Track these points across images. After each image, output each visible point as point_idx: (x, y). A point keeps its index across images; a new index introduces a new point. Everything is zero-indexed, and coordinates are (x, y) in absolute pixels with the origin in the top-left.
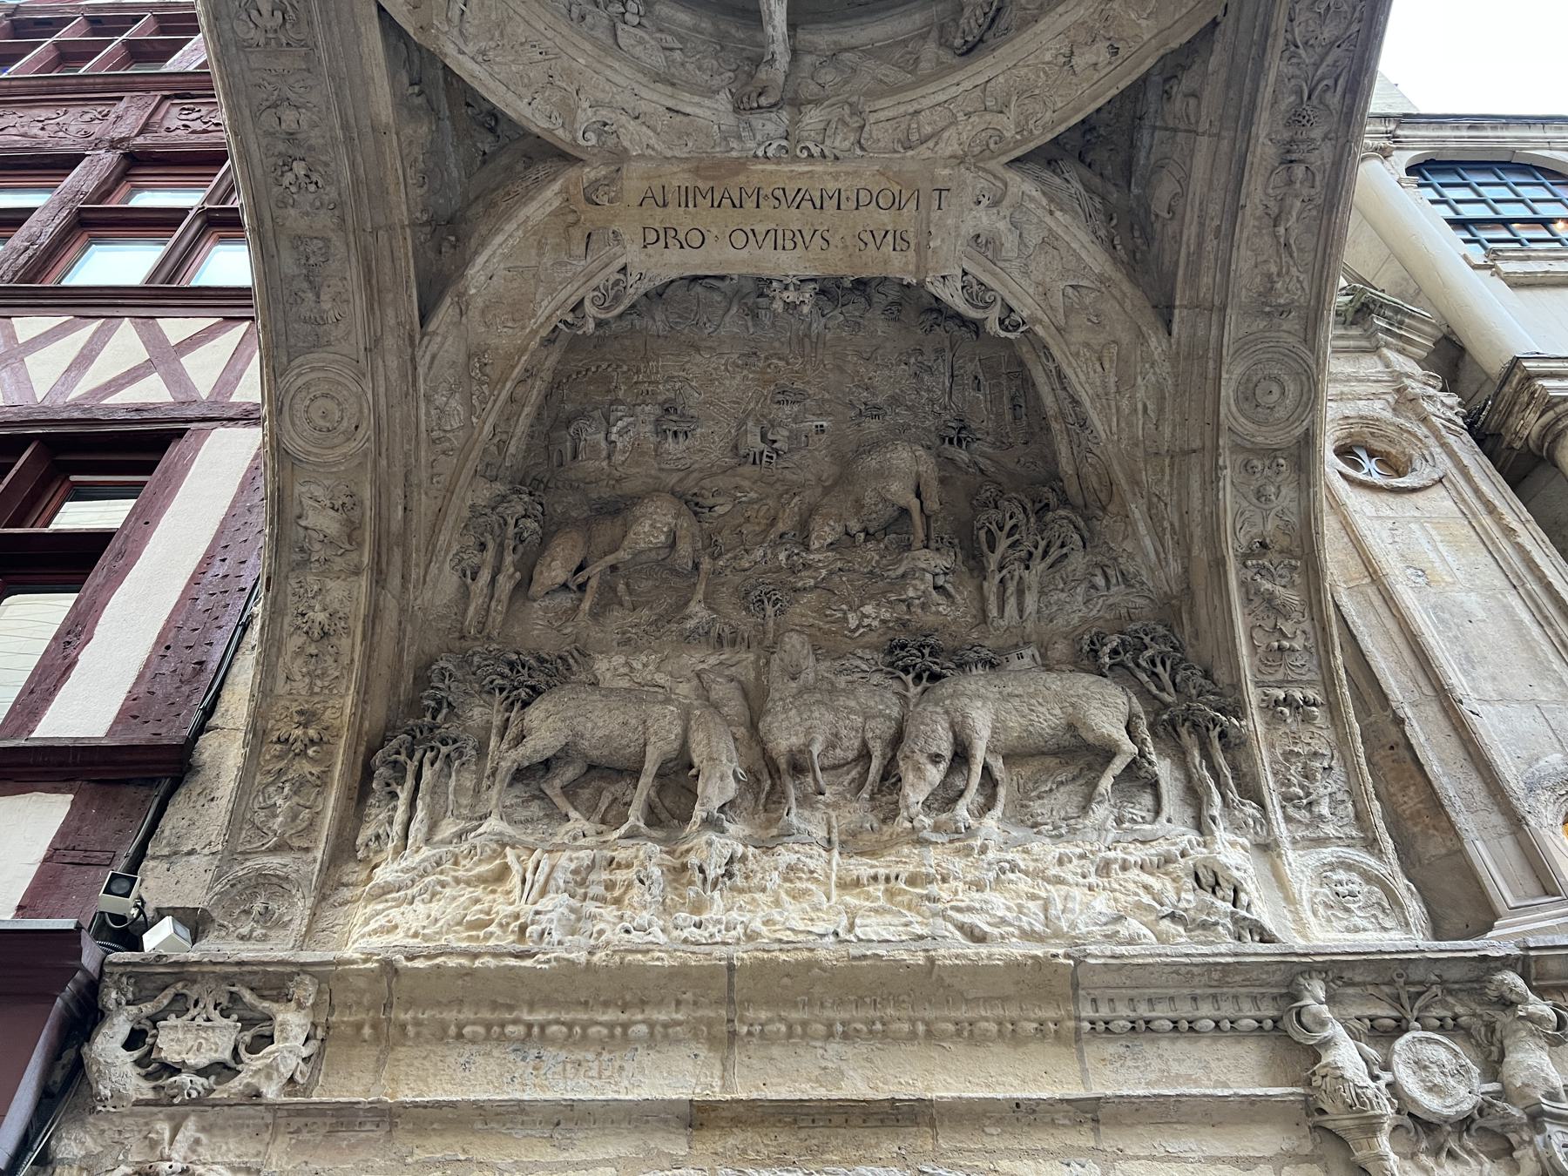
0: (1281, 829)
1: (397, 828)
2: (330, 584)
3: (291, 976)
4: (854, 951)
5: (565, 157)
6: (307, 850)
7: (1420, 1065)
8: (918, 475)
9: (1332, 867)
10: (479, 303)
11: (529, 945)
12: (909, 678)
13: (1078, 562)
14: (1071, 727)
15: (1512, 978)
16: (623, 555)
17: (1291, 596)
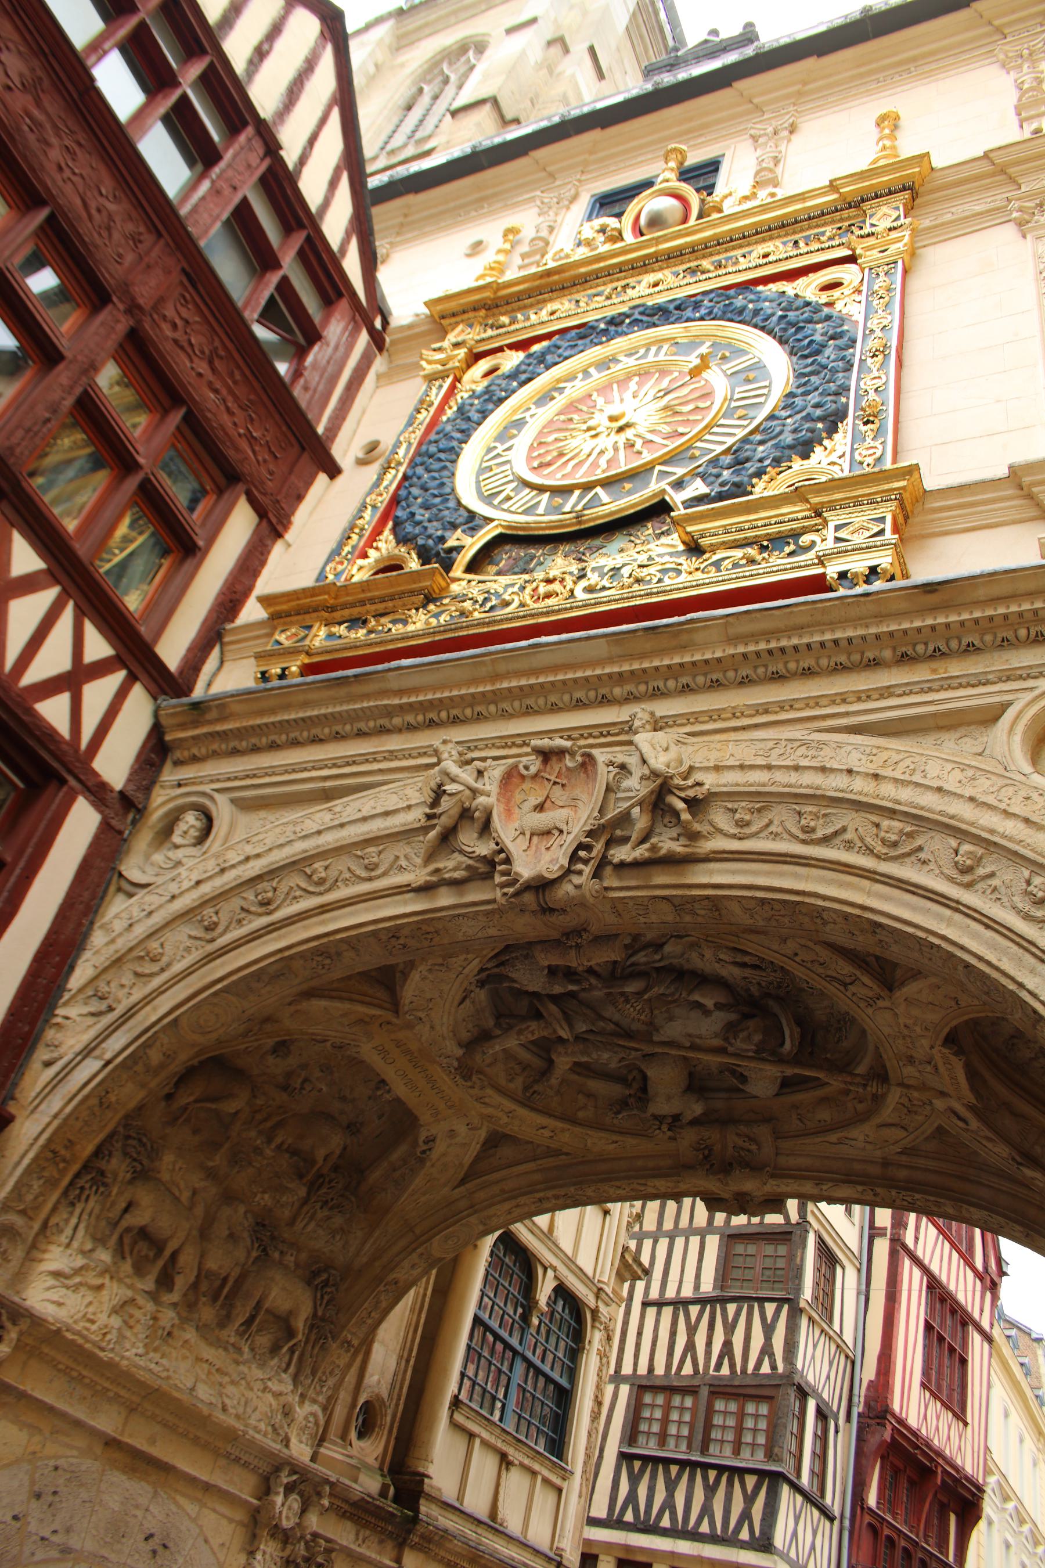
0: (311, 1393)
1: (68, 1231)
2: (130, 1085)
3: (23, 1316)
4: (194, 1402)
5: (395, 1007)
6: (31, 1219)
7: (290, 1508)
8: (332, 1153)
9: (311, 1414)
10: (299, 1007)
11: (104, 1344)
12: (256, 1245)
13: (338, 1220)
14: (290, 1312)
15: (327, 1488)
16: (214, 1106)
17: (384, 1305)
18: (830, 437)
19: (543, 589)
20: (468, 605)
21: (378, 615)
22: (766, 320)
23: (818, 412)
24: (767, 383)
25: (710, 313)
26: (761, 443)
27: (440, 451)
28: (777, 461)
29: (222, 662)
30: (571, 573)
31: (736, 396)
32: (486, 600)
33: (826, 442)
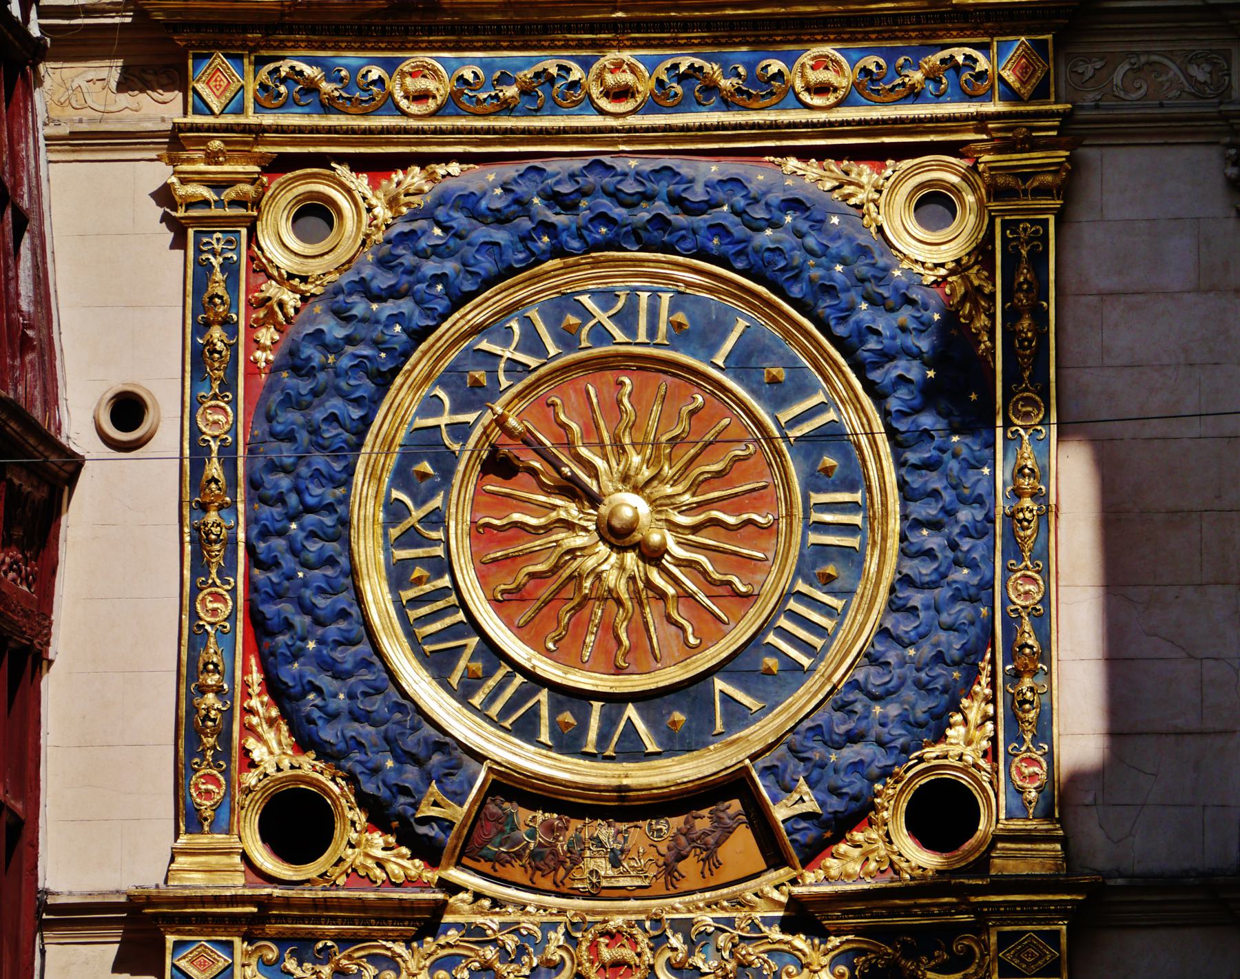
18: (970, 695)
19: (606, 954)
20: (490, 953)
21: (344, 941)
22: (842, 320)
23: (954, 644)
24: (858, 497)
25: (739, 253)
26: (876, 698)
27: (309, 509)
28: (906, 750)
29: (43, 952)
30: (640, 923)
31: (815, 516)
32: (521, 950)
33: (965, 702)
